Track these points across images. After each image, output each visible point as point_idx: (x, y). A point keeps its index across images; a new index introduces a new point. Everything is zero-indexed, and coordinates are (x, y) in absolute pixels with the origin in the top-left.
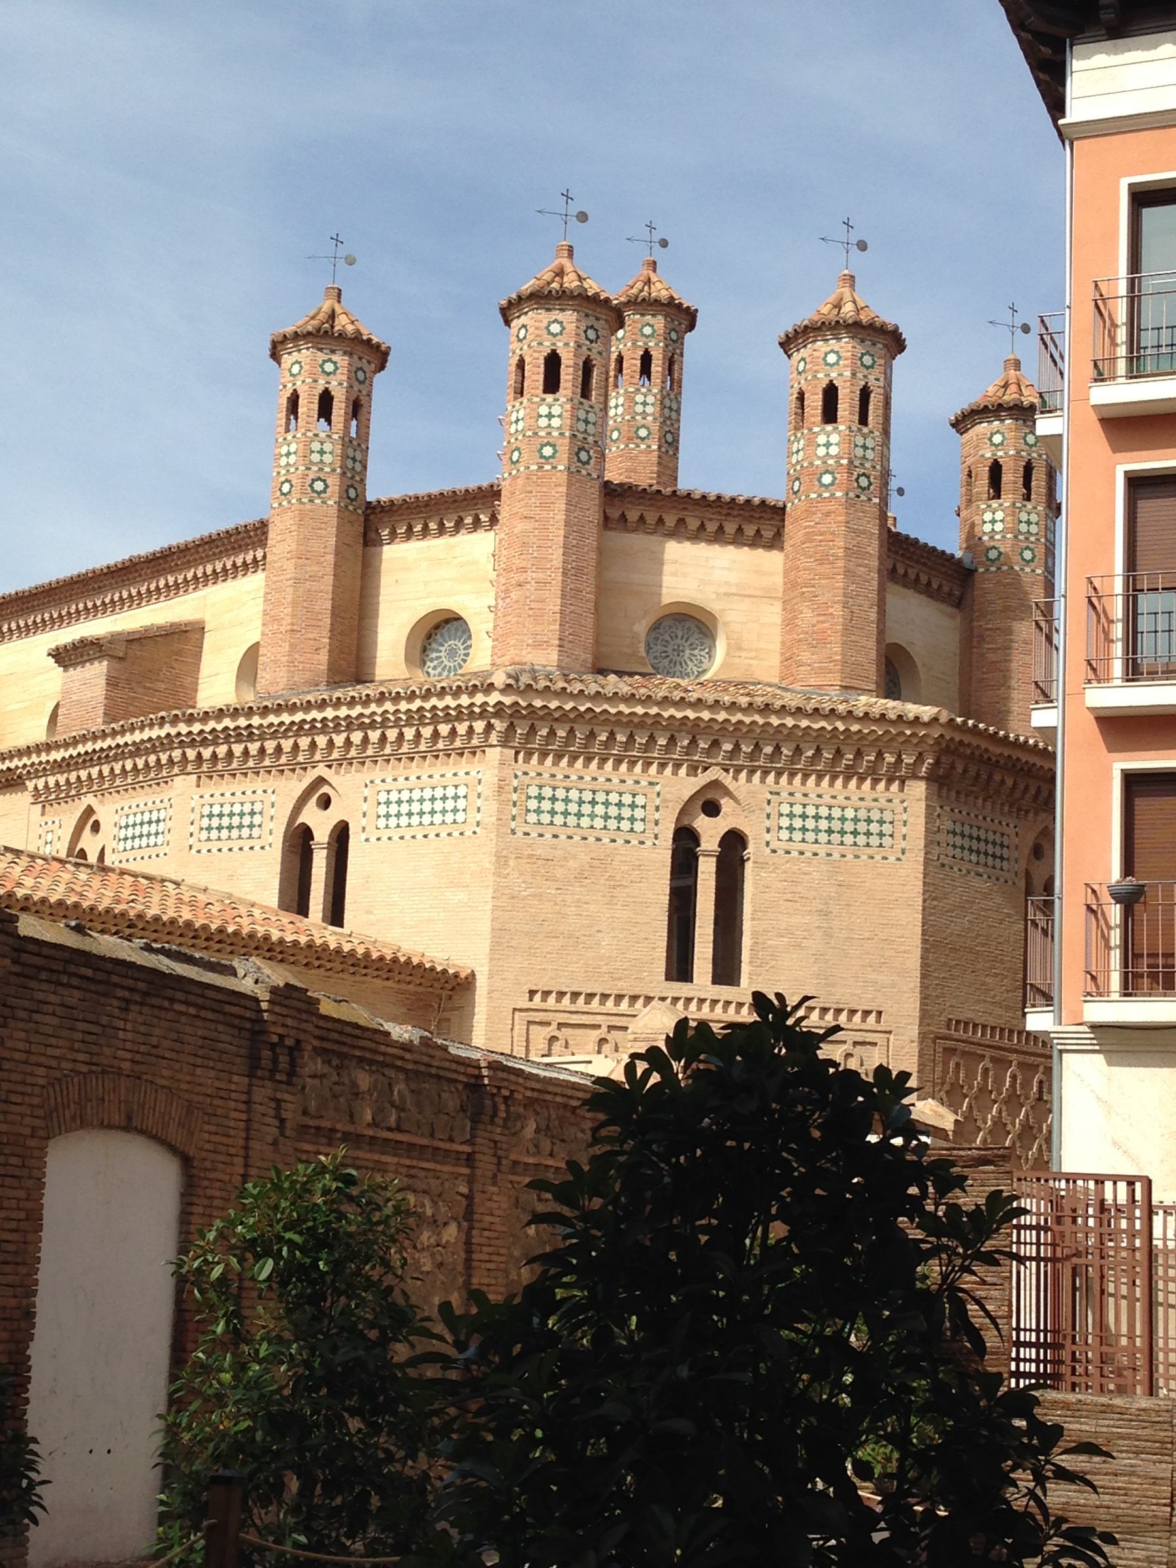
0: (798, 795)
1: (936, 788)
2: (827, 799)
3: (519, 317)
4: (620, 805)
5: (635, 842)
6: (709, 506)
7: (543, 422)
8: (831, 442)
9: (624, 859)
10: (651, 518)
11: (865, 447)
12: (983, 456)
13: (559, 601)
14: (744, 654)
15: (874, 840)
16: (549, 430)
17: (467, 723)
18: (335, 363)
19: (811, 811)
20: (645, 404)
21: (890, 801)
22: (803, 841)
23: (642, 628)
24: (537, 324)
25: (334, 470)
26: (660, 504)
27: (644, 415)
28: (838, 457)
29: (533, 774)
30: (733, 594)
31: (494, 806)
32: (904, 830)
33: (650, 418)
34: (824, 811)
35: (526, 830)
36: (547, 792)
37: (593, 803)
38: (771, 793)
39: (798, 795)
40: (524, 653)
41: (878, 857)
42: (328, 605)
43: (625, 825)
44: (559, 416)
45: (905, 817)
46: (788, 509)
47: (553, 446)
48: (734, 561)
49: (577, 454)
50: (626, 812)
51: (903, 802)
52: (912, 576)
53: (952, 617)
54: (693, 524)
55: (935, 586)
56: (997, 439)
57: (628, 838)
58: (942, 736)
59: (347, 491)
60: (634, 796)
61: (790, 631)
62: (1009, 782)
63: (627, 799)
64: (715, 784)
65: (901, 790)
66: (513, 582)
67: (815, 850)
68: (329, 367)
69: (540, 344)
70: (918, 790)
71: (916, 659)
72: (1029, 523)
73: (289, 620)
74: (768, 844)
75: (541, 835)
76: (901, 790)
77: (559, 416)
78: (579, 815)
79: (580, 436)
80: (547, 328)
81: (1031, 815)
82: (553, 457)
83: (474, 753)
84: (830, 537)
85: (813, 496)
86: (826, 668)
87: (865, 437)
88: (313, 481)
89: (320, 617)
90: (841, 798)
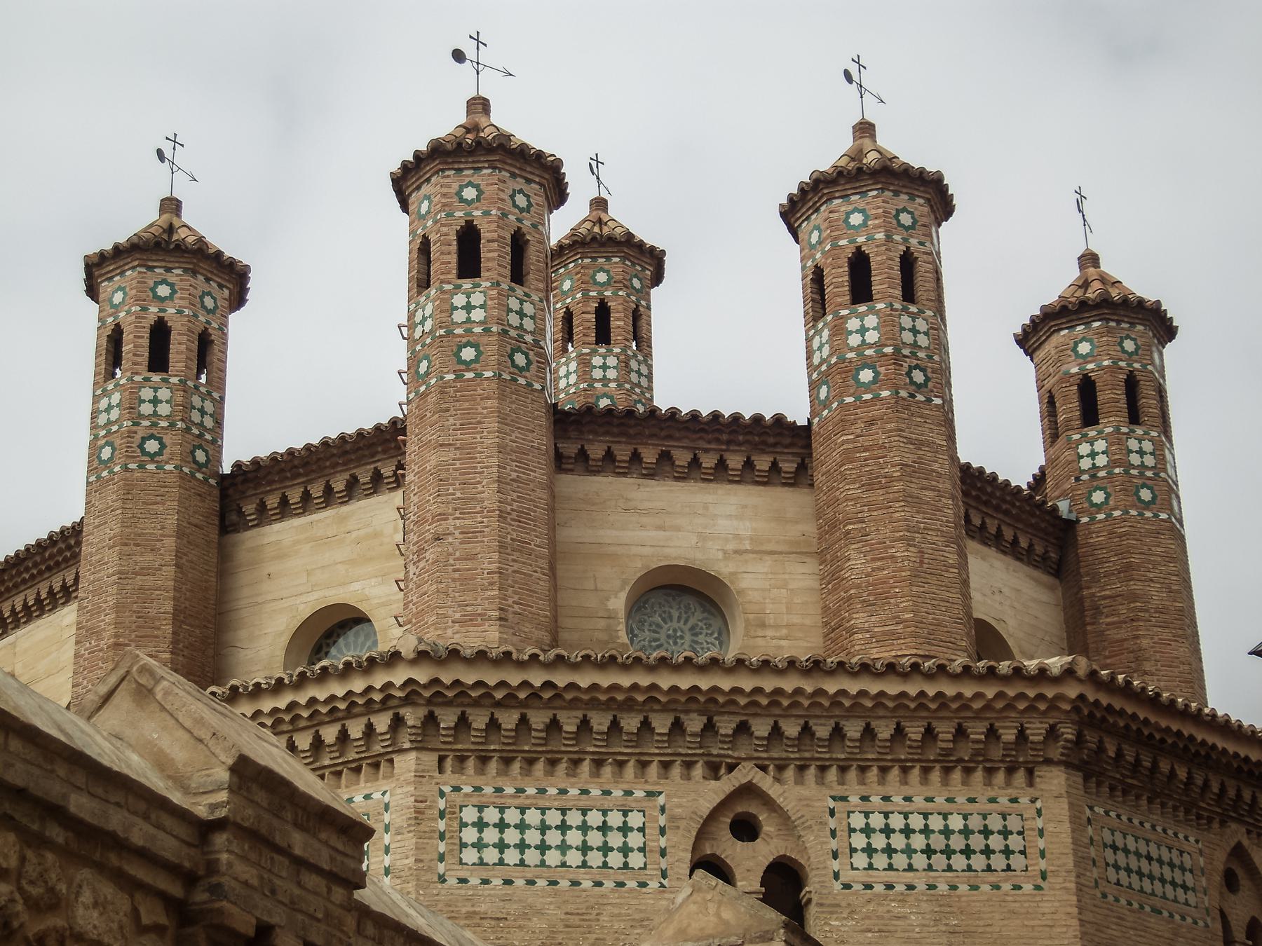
0: (875, 799)
1: (1080, 780)
2: (919, 801)
3: (418, 188)
4: (604, 828)
5: (632, 884)
6: (702, 430)
7: (460, 316)
8: (865, 327)
9: (616, 911)
10: (623, 453)
11: (914, 331)
12: (1067, 373)
13: (496, 556)
14: (770, 633)
15: (998, 861)
16: (468, 326)
17: (364, 720)
18: (172, 285)
19: (897, 822)
20: (604, 367)
21: (1014, 800)
22: (890, 867)
23: (619, 603)
24: (445, 190)
25: (172, 425)
26: (632, 431)
27: (605, 382)
28: (879, 345)
29: (467, 789)
30: (746, 551)
31: (410, 841)
32: (1041, 843)
33: (613, 385)
34: (916, 822)
35: (462, 874)
36: (492, 815)
37: (563, 827)
38: (834, 798)
39: (875, 799)
40: (449, 632)
41: (1006, 887)
42: (168, 606)
43: (615, 859)
44: (481, 307)
45: (1040, 823)
46: (815, 427)
47: (475, 346)
48: (745, 506)
49: (511, 357)
50: (615, 840)
51: (1033, 801)
52: (993, 530)
53: (1052, 588)
54: (682, 458)
55: (1024, 543)
56: (1084, 348)
57: (621, 878)
58: (1081, 697)
59: (193, 452)
60: (625, 814)
61: (834, 589)
62: (1182, 774)
63: (615, 819)
64: (748, 791)
65: (1031, 784)
66: (429, 536)
67: (908, 881)
68: (163, 291)
69: (449, 215)
70: (1055, 781)
71: (1011, 643)
72: (1141, 453)
73: (111, 630)
74: (836, 876)
75: (485, 882)
76: (1031, 784)
77: (481, 307)
78: (543, 848)
79: (513, 333)
80: (459, 194)
81: (1216, 825)
82: (476, 360)
83: (376, 766)
84: (877, 452)
85: (849, 400)
86: (892, 633)
87: (914, 317)
88: (144, 439)
89: (157, 623)
90: (940, 800)
